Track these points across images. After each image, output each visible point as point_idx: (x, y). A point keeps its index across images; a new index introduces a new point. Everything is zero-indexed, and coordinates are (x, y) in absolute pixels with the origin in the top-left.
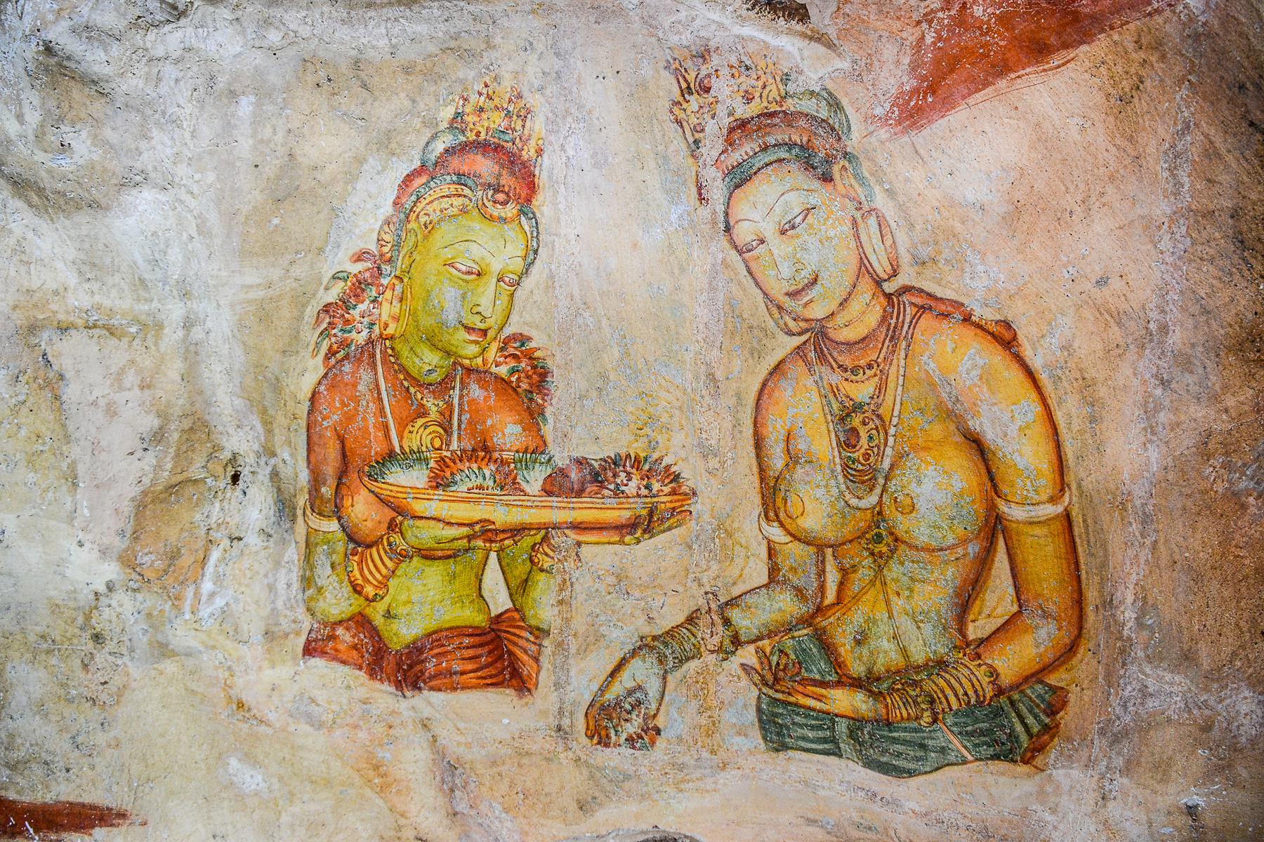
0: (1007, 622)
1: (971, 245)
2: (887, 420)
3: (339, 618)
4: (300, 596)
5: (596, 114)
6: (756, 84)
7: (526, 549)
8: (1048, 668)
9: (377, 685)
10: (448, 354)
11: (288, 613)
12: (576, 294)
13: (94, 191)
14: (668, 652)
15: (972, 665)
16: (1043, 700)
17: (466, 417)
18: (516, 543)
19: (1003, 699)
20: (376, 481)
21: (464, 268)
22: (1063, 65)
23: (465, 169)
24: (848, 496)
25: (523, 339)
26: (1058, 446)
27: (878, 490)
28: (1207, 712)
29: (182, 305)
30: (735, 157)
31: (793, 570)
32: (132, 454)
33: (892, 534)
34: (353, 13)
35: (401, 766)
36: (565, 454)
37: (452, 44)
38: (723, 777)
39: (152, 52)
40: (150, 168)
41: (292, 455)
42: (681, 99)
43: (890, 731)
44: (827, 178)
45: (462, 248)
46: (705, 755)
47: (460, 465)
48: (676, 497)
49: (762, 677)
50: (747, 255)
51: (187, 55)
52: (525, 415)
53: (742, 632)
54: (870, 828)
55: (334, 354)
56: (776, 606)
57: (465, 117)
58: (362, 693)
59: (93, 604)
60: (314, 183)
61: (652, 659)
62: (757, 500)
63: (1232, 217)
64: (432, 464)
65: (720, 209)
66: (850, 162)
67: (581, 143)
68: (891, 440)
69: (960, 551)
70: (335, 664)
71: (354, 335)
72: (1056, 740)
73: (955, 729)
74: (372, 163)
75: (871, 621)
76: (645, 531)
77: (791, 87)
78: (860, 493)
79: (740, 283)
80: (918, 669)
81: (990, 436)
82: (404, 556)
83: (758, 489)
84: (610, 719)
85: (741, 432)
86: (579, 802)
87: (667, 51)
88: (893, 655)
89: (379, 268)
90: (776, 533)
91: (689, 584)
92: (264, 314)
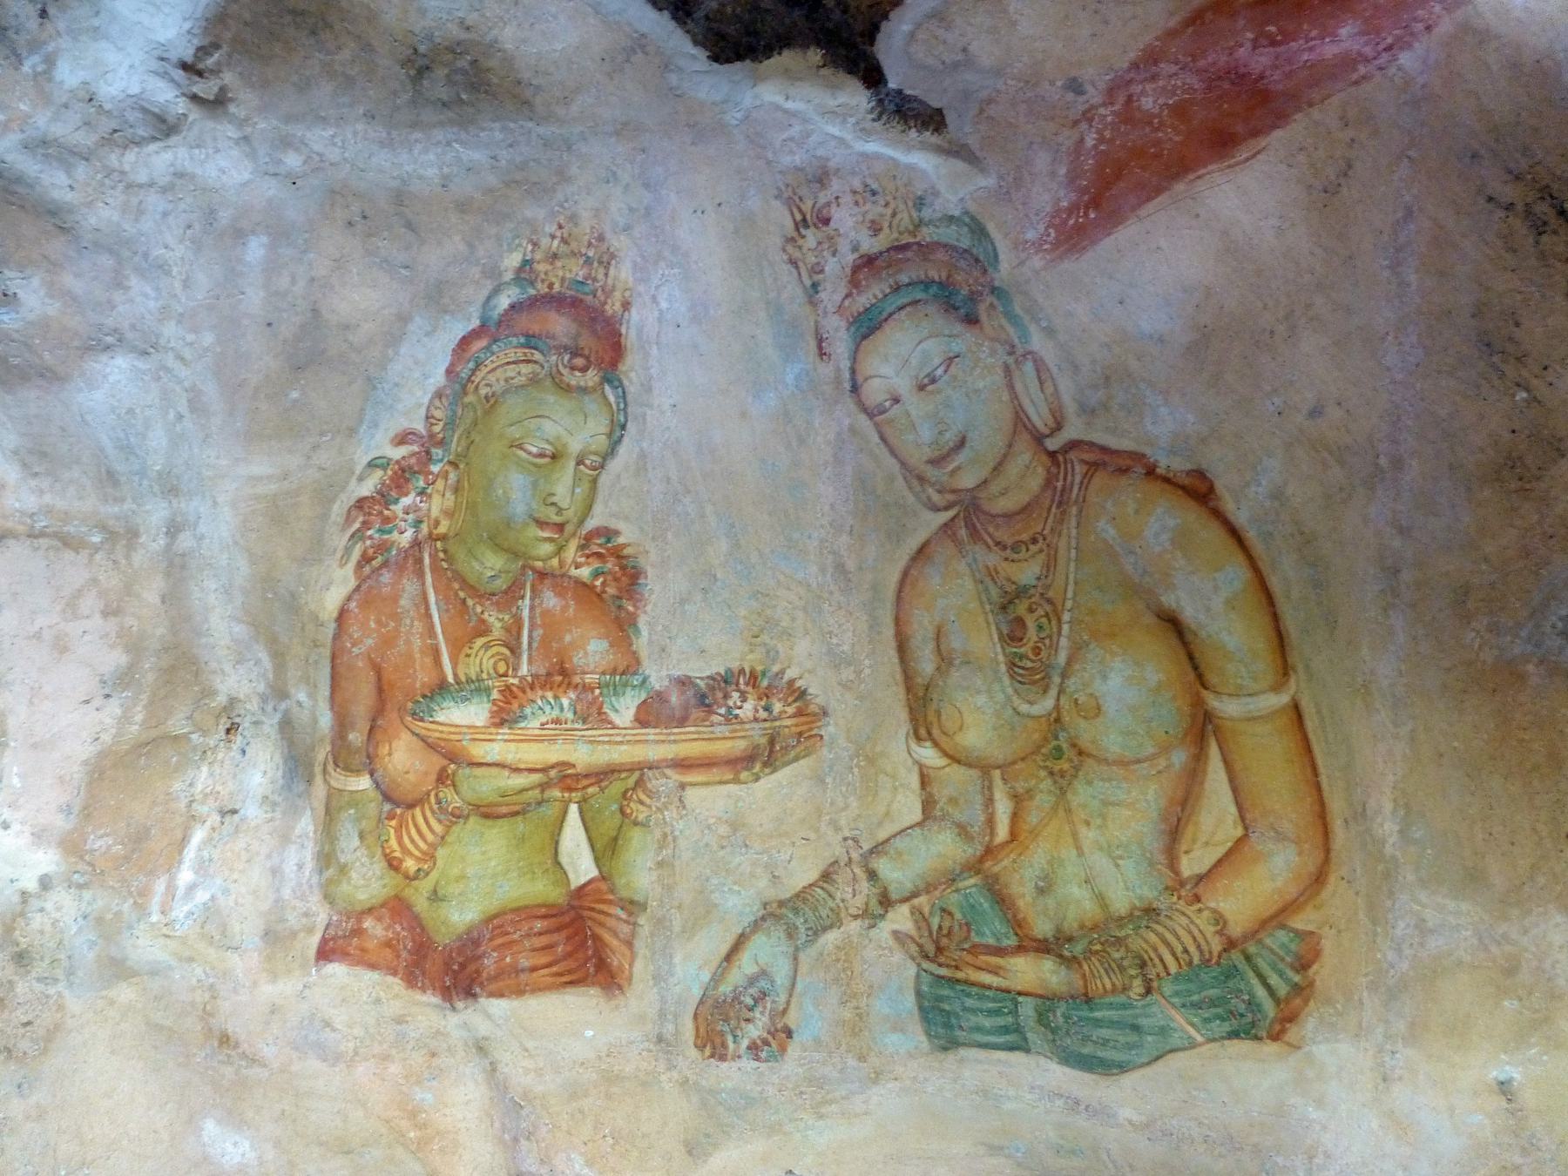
0: (1229, 854)
3: (368, 905)
4: (315, 880)
10: (515, 554)
11: (298, 904)
13: (47, 356)
14: (799, 921)
16: (1289, 951)
17: (539, 632)
18: (602, 790)
19: (1236, 956)
20: (422, 720)
21: (534, 450)
22: (1254, 156)
23: (535, 328)
24: (1016, 701)
25: (608, 533)
26: (1275, 617)
27: (1053, 692)
29: (165, 505)
30: (863, 301)
31: (952, 801)
32: (87, 702)
33: (1074, 745)
34: (394, 133)
35: (447, 1111)
36: (664, 673)
37: (518, 177)
39: (132, 177)
41: (311, 696)
42: (795, 234)
43: (1091, 1010)
45: (532, 426)
46: (851, 1062)
47: (530, 694)
49: (920, 946)
51: (179, 182)
53: (892, 888)
54: (1073, 1152)
58: (394, 1008)
59: (19, 908)
61: (779, 933)
62: (903, 715)
63: (1473, 316)
64: (495, 695)
65: (845, 364)
66: (999, 298)
67: (677, 293)
68: (1066, 628)
70: (359, 970)
71: (395, 534)
72: (1312, 1003)
74: (419, 323)
77: (926, 213)
78: (1031, 697)
80: (1120, 921)
81: (1189, 613)
82: (457, 816)
83: (903, 703)
85: (879, 633)
86: (686, 1143)
87: (779, 177)
89: (428, 453)
90: (928, 754)
91: (823, 828)
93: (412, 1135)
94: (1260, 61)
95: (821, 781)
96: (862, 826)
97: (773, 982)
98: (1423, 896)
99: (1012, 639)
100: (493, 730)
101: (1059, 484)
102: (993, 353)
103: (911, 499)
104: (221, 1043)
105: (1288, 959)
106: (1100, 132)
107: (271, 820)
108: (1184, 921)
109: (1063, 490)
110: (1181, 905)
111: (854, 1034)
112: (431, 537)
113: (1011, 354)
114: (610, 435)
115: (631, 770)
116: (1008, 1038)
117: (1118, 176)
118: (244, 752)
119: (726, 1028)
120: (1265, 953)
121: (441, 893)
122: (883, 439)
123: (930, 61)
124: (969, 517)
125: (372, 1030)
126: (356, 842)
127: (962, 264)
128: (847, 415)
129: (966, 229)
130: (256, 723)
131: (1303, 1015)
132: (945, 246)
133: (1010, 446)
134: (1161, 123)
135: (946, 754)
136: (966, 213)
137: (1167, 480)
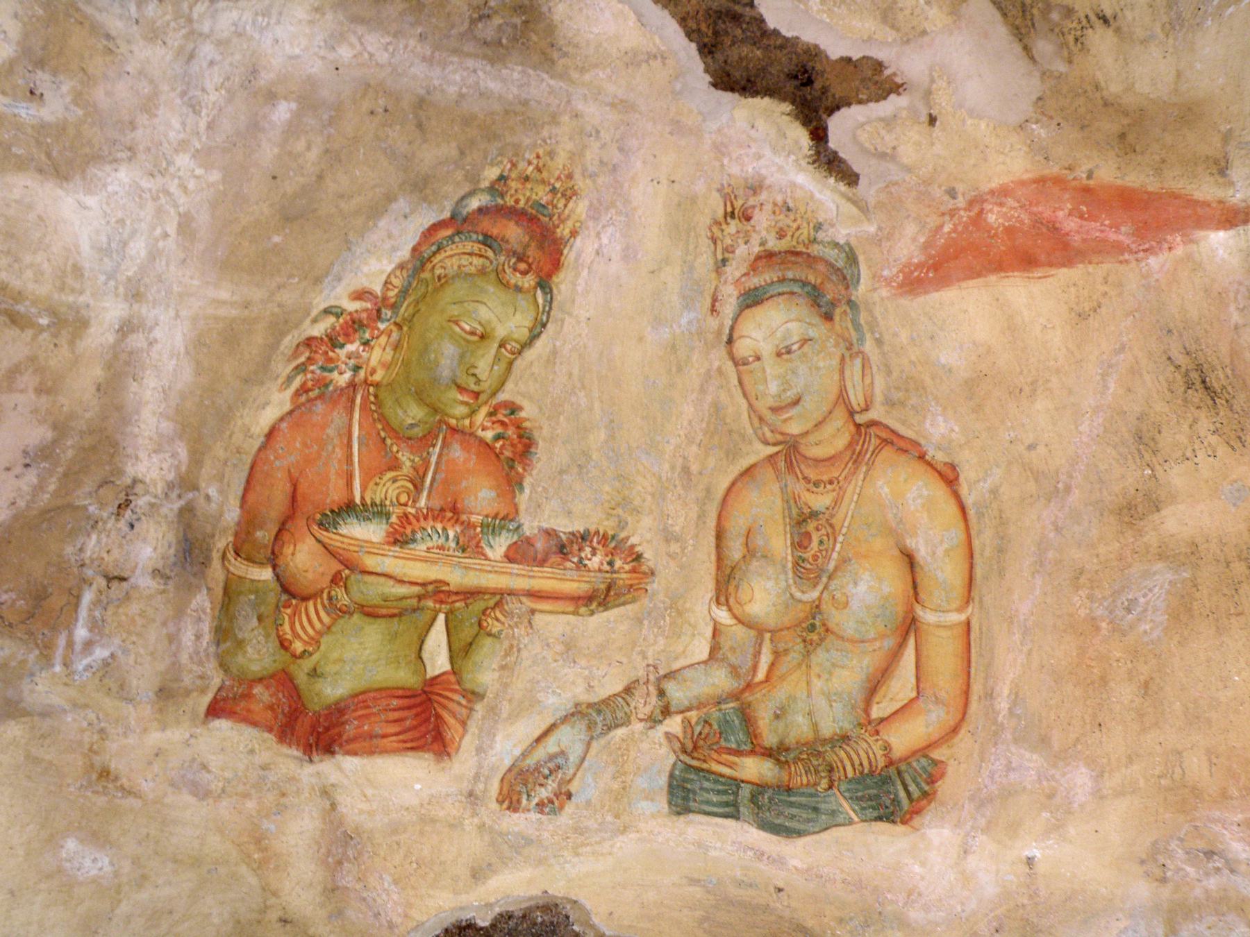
1: (936, 398)
2: (837, 528)
3: (260, 675)
4: (212, 649)
5: (640, 212)
7: (473, 615)
9: (285, 750)
10: (435, 410)
11: (195, 668)
12: (576, 372)
14: (599, 719)
15: (871, 740)
18: (467, 606)
19: (892, 770)
20: (327, 530)
21: (467, 328)
23: (495, 232)
24: (794, 590)
25: (513, 409)
27: (820, 587)
28: (1054, 783)
30: (756, 281)
31: (733, 649)
32: (8, 469)
33: (824, 625)
35: (284, 839)
36: (536, 524)
37: (519, 108)
38: (621, 841)
39: (196, 26)
40: (141, 147)
41: (221, 492)
42: (722, 220)
44: (828, 317)
45: (470, 308)
46: (609, 818)
47: (423, 524)
50: (741, 368)
51: (235, 40)
53: (673, 703)
54: (751, 885)
55: (307, 391)
57: (509, 182)
58: (264, 757)
61: (581, 725)
62: (711, 585)
65: (728, 323)
67: (618, 235)
68: (838, 546)
71: (335, 374)
72: (933, 804)
74: (402, 204)
75: (792, 698)
76: (600, 604)
77: (821, 235)
80: (824, 741)
81: (922, 552)
82: (345, 612)
86: (473, 869)
88: (805, 729)
89: (379, 311)
90: (723, 615)
91: (635, 655)
92: (231, 335)
93: (256, 856)
94: (1071, 225)
95: (640, 621)
96: (663, 659)
97: (567, 759)
98: (1013, 749)
100: (387, 547)
101: (858, 448)
102: (837, 345)
104: (100, 776)
107: (164, 592)
108: (865, 745)
109: (860, 453)
111: (616, 800)
113: (849, 349)
114: (531, 330)
115: (494, 594)
116: (727, 809)
118: (132, 526)
121: (318, 671)
122: (740, 383)
123: (867, 145)
124: (790, 454)
125: (240, 774)
126: (255, 622)
127: (834, 278)
128: (718, 356)
129: (844, 255)
130: (152, 505)
134: (996, 234)
135: (735, 617)
136: (848, 244)
137: (929, 464)
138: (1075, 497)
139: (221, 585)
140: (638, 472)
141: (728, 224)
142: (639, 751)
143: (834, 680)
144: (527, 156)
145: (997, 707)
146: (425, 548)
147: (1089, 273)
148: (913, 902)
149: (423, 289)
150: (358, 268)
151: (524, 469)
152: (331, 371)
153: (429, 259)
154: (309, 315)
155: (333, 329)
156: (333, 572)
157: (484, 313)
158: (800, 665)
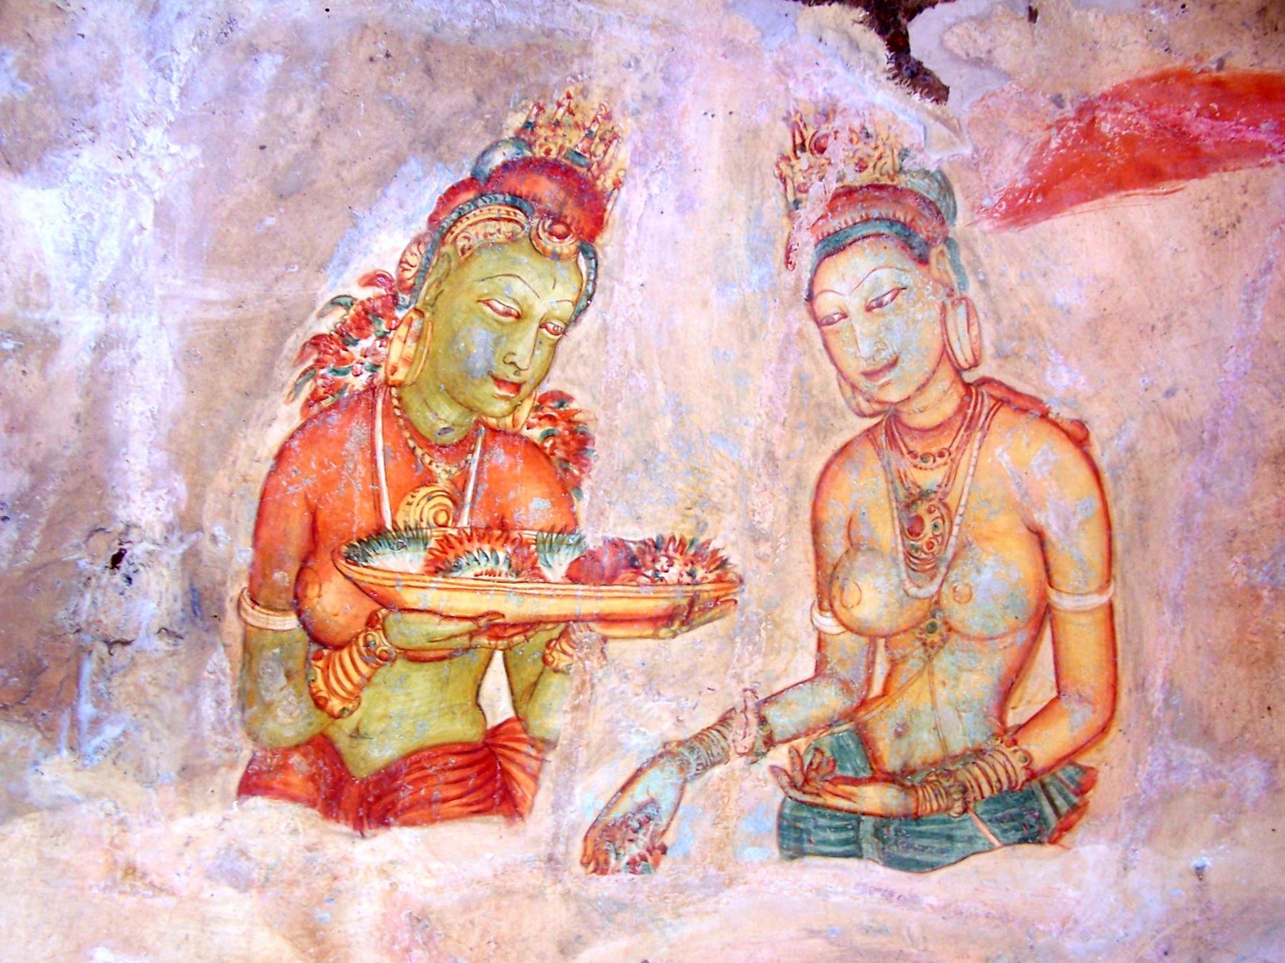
1: (1055, 345)
2: (953, 508)
3: (294, 742)
4: (237, 716)
5: (694, 152)
6: (872, 153)
8: (1080, 750)
11: (220, 739)
12: (632, 349)
14: (692, 758)
15: (1008, 751)
16: (1073, 781)
17: (484, 487)
18: (527, 639)
19: (1035, 784)
20: (356, 564)
21: (501, 308)
23: (524, 190)
24: (908, 585)
25: (562, 398)
26: (1110, 540)
27: (938, 580)
28: (1222, 781)
29: (101, 318)
31: (841, 662)
33: (946, 623)
36: (600, 535)
37: (543, 41)
38: (726, 896)
40: (105, 125)
41: (229, 530)
43: (918, 825)
44: (923, 261)
46: (712, 871)
47: (467, 545)
48: (721, 585)
49: (791, 779)
50: (826, 328)
52: (558, 489)
54: (880, 931)
56: (818, 701)
57: (537, 130)
60: (334, 180)
62: (811, 589)
64: (432, 544)
65: (807, 276)
66: (949, 247)
67: (670, 182)
68: (956, 529)
69: (1009, 640)
72: (1084, 818)
73: (984, 817)
74: (413, 167)
75: (914, 712)
77: (907, 164)
78: (920, 583)
79: (813, 357)
80: (955, 758)
81: (1053, 531)
82: (386, 659)
84: (612, 841)
85: (797, 516)
86: (560, 943)
87: (792, 103)
89: (395, 297)
90: (827, 623)
92: (225, 343)
93: (312, 950)
95: (731, 639)
96: (760, 680)
98: (1172, 745)
99: (911, 533)
100: (427, 578)
101: (970, 411)
102: (935, 293)
103: (841, 402)
104: (126, 874)
105: (1072, 787)
106: (1064, 139)
107: (173, 654)
108: (1002, 758)
109: (972, 418)
110: (1003, 748)
111: (719, 849)
112: (387, 384)
113: (949, 296)
114: (575, 303)
115: (557, 622)
116: (847, 848)
117: (1067, 177)
118: (129, 580)
119: (611, 848)
120: (1056, 782)
121: (361, 731)
123: (957, 51)
124: (891, 427)
126: (283, 680)
127: (927, 213)
129: (936, 185)
130: (150, 553)
131: (1075, 827)
132: (916, 194)
133: (934, 372)
134: (1112, 147)
136: (940, 171)
137: (1055, 424)
138: (1224, 448)
139: (239, 640)
140: (715, 462)
141: (798, 158)
142: (741, 790)
143: (961, 686)
144: (556, 97)
145: (1150, 699)
146: (471, 574)
147: (1224, 183)
148: (1069, 930)
149: (445, 265)
150: (367, 247)
151: (581, 471)
152: (345, 373)
153: (449, 230)
154: (313, 308)
155: (344, 323)
156: (368, 613)
157: (519, 288)
158: (920, 673)
